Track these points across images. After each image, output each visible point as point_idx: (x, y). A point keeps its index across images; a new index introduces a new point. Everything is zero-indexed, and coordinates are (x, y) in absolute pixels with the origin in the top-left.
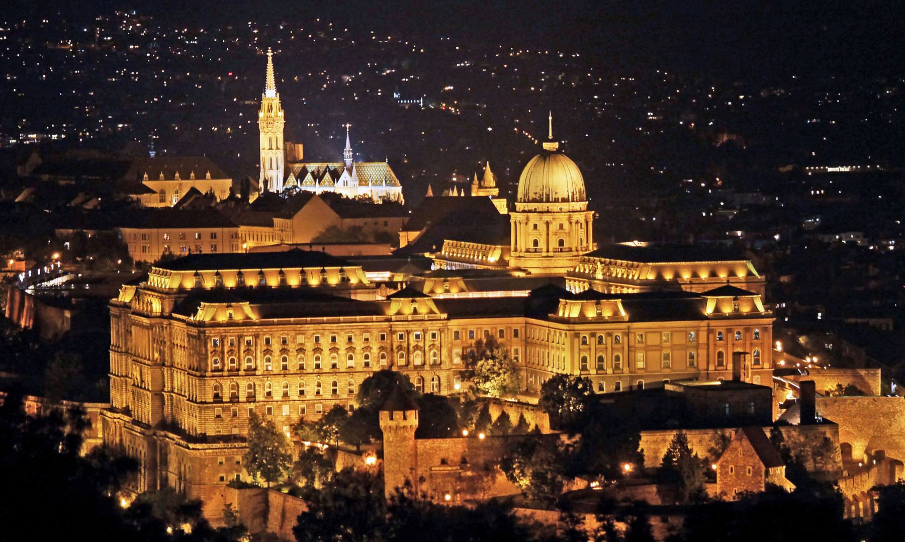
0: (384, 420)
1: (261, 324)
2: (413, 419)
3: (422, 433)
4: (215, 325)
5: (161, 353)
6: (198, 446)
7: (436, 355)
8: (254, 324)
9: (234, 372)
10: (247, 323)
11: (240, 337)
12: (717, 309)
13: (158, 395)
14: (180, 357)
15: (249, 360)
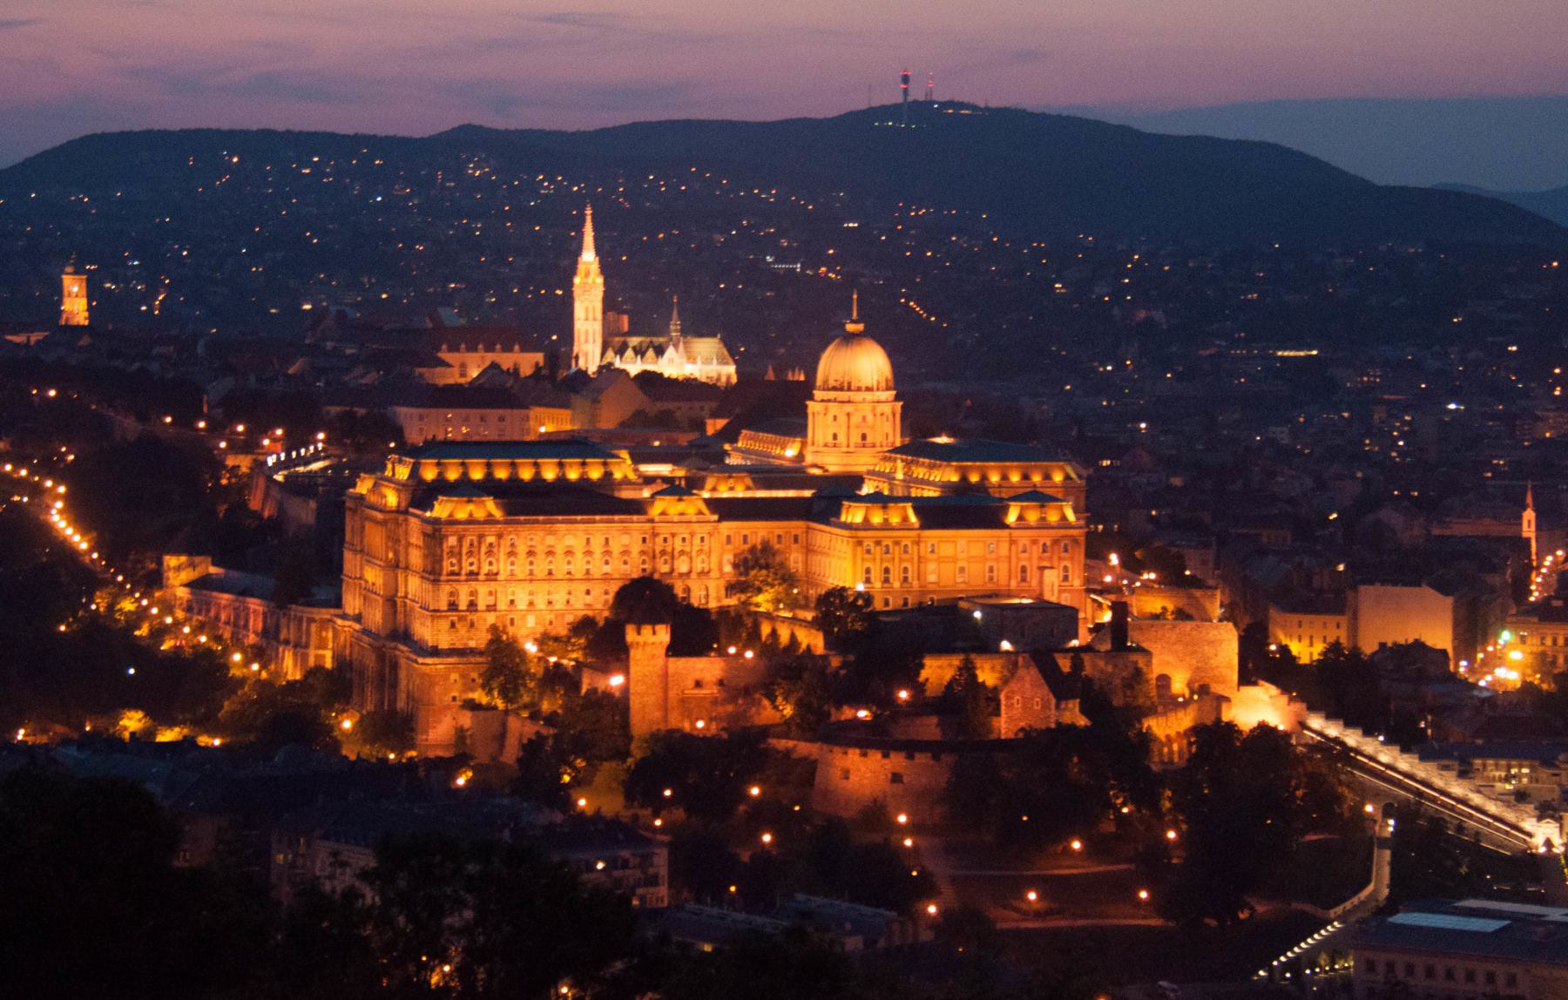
0: (631, 635)
1: (506, 522)
2: (663, 635)
3: (674, 650)
4: (452, 522)
5: (396, 553)
6: (429, 661)
7: (704, 560)
8: (497, 522)
9: (473, 576)
10: (490, 520)
11: (481, 537)
12: (1020, 518)
13: (391, 601)
14: (416, 558)
15: (491, 563)
